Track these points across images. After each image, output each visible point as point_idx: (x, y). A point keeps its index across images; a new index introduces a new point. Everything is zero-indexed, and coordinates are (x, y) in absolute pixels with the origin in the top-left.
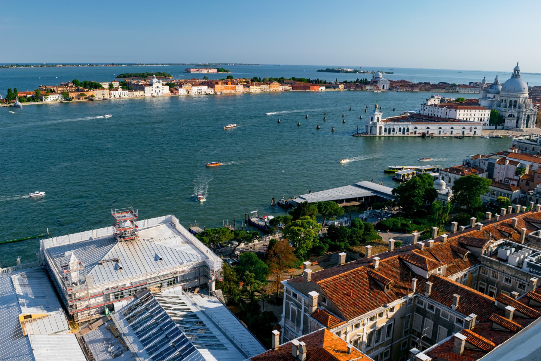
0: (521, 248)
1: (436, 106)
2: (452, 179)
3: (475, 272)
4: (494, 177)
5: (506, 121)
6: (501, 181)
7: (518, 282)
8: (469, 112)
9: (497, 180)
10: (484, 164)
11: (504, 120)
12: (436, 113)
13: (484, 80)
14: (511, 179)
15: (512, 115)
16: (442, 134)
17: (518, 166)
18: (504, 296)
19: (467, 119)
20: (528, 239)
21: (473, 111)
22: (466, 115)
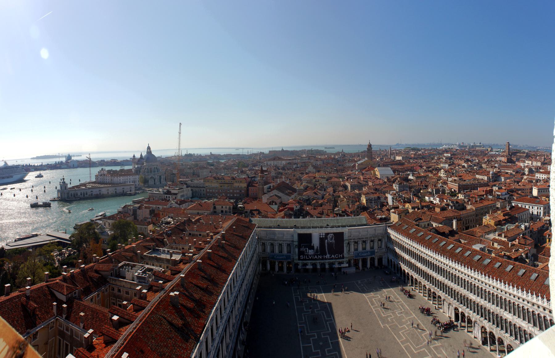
0: (134, 266)
1: (104, 175)
2: (111, 224)
3: (106, 290)
4: (138, 218)
5: (149, 181)
6: (142, 220)
7: (134, 292)
8: (126, 178)
9: (140, 220)
10: (131, 211)
11: (148, 180)
12: (105, 180)
13: (134, 156)
14: (147, 218)
15: (152, 177)
16: (110, 193)
17: (151, 209)
18: (114, 307)
19: (125, 182)
20: (144, 258)
21: (129, 177)
22: (124, 180)
